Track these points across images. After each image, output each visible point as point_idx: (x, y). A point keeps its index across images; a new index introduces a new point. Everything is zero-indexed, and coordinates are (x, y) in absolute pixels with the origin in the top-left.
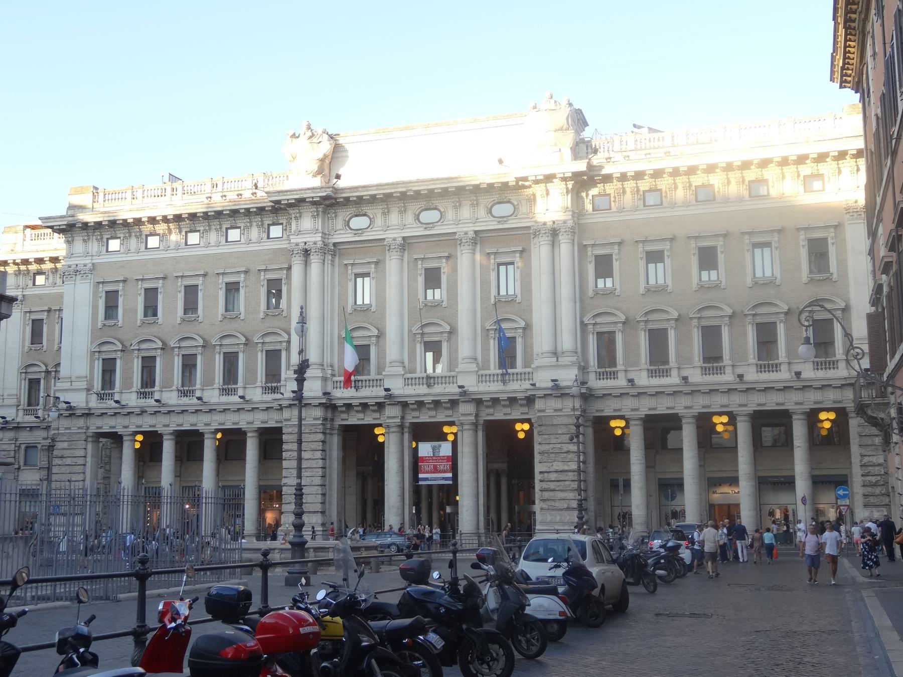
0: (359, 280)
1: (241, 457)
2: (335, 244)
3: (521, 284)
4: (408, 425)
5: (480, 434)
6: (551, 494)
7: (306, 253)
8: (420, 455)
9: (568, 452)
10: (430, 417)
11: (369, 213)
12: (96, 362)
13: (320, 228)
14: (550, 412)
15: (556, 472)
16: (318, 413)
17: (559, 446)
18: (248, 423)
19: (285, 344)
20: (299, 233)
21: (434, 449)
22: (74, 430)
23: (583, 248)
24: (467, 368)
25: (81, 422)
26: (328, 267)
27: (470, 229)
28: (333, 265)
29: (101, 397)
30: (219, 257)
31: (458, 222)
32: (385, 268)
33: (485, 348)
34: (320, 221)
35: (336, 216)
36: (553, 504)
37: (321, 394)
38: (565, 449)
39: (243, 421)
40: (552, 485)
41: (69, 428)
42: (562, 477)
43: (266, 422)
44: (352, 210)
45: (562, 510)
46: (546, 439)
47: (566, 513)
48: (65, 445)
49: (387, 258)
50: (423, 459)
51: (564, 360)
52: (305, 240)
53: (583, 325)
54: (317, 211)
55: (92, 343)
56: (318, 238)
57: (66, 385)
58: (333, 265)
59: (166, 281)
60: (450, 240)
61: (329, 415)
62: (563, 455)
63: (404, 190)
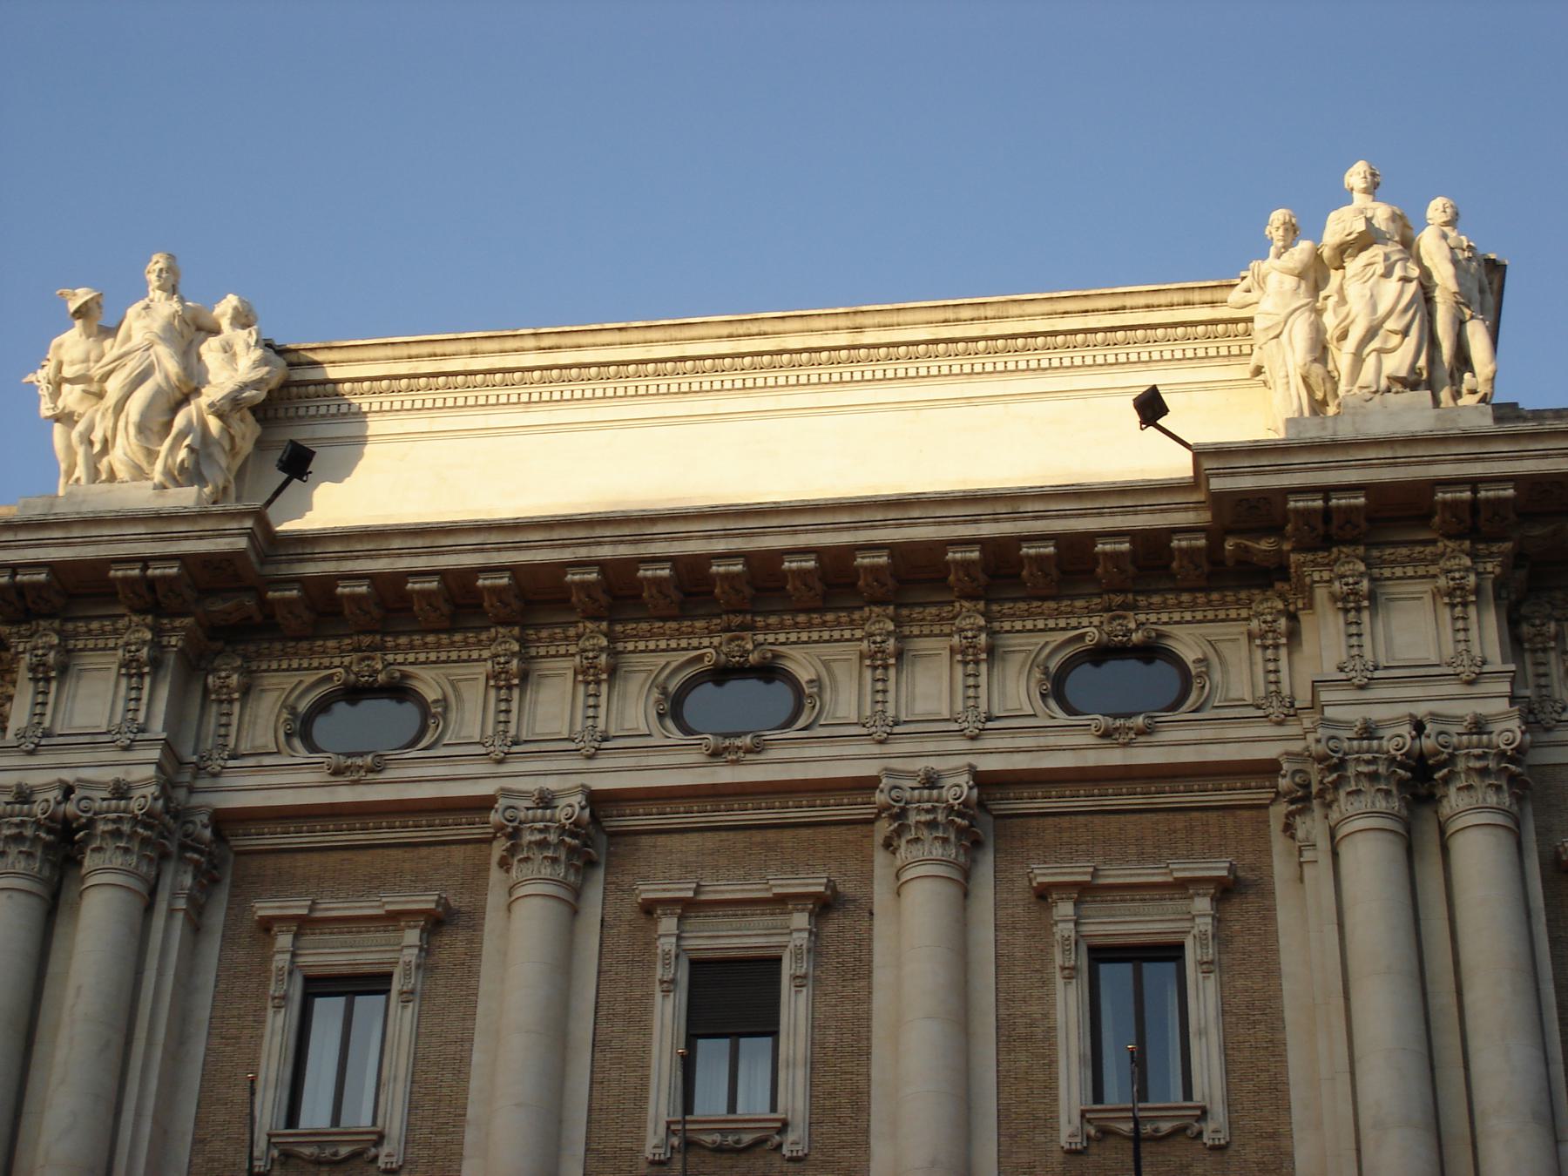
0: (328, 1011)
2: (225, 821)
3: (1227, 1049)
13: (158, 728)
26: (168, 930)
28: (196, 926)
31: (886, 730)
32: (474, 954)
35: (246, 691)
44: (340, 662)
49: (495, 899)
52: (68, 776)
54: (157, 645)
56: (141, 769)
58: (196, 926)
60: (850, 813)
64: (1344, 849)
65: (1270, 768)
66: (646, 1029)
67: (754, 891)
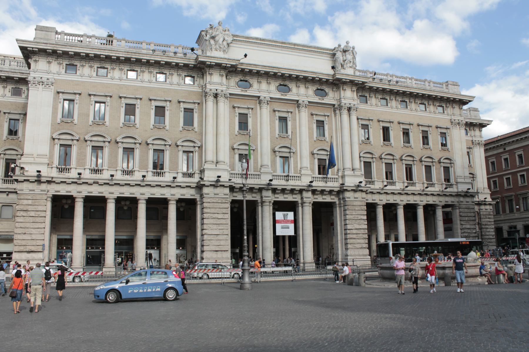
1: (134, 217)
2: (230, 94)
3: (329, 132)
6: (354, 240)
7: (216, 96)
10: (285, 198)
11: (251, 81)
12: (56, 145)
14: (352, 199)
15: (356, 229)
16: (227, 191)
17: (357, 216)
18: (172, 195)
19: (197, 148)
20: (214, 83)
21: (284, 215)
22: (37, 191)
23: (358, 119)
24: (304, 172)
25: (44, 186)
26: (226, 106)
27: (306, 100)
29: (61, 170)
30: (151, 89)
33: (312, 164)
34: (224, 78)
37: (228, 181)
38: (360, 218)
39: (166, 193)
40: (354, 236)
41: (34, 190)
43: (184, 195)
47: (361, 250)
48: (30, 202)
50: (279, 222)
51: (357, 173)
52: (217, 88)
53: (360, 157)
55: (52, 133)
57: (31, 160)
59: (112, 99)
62: (358, 221)
63: (277, 71)
64: (342, 116)
65: (334, 105)
66: (275, 124)
67: (286, 110)
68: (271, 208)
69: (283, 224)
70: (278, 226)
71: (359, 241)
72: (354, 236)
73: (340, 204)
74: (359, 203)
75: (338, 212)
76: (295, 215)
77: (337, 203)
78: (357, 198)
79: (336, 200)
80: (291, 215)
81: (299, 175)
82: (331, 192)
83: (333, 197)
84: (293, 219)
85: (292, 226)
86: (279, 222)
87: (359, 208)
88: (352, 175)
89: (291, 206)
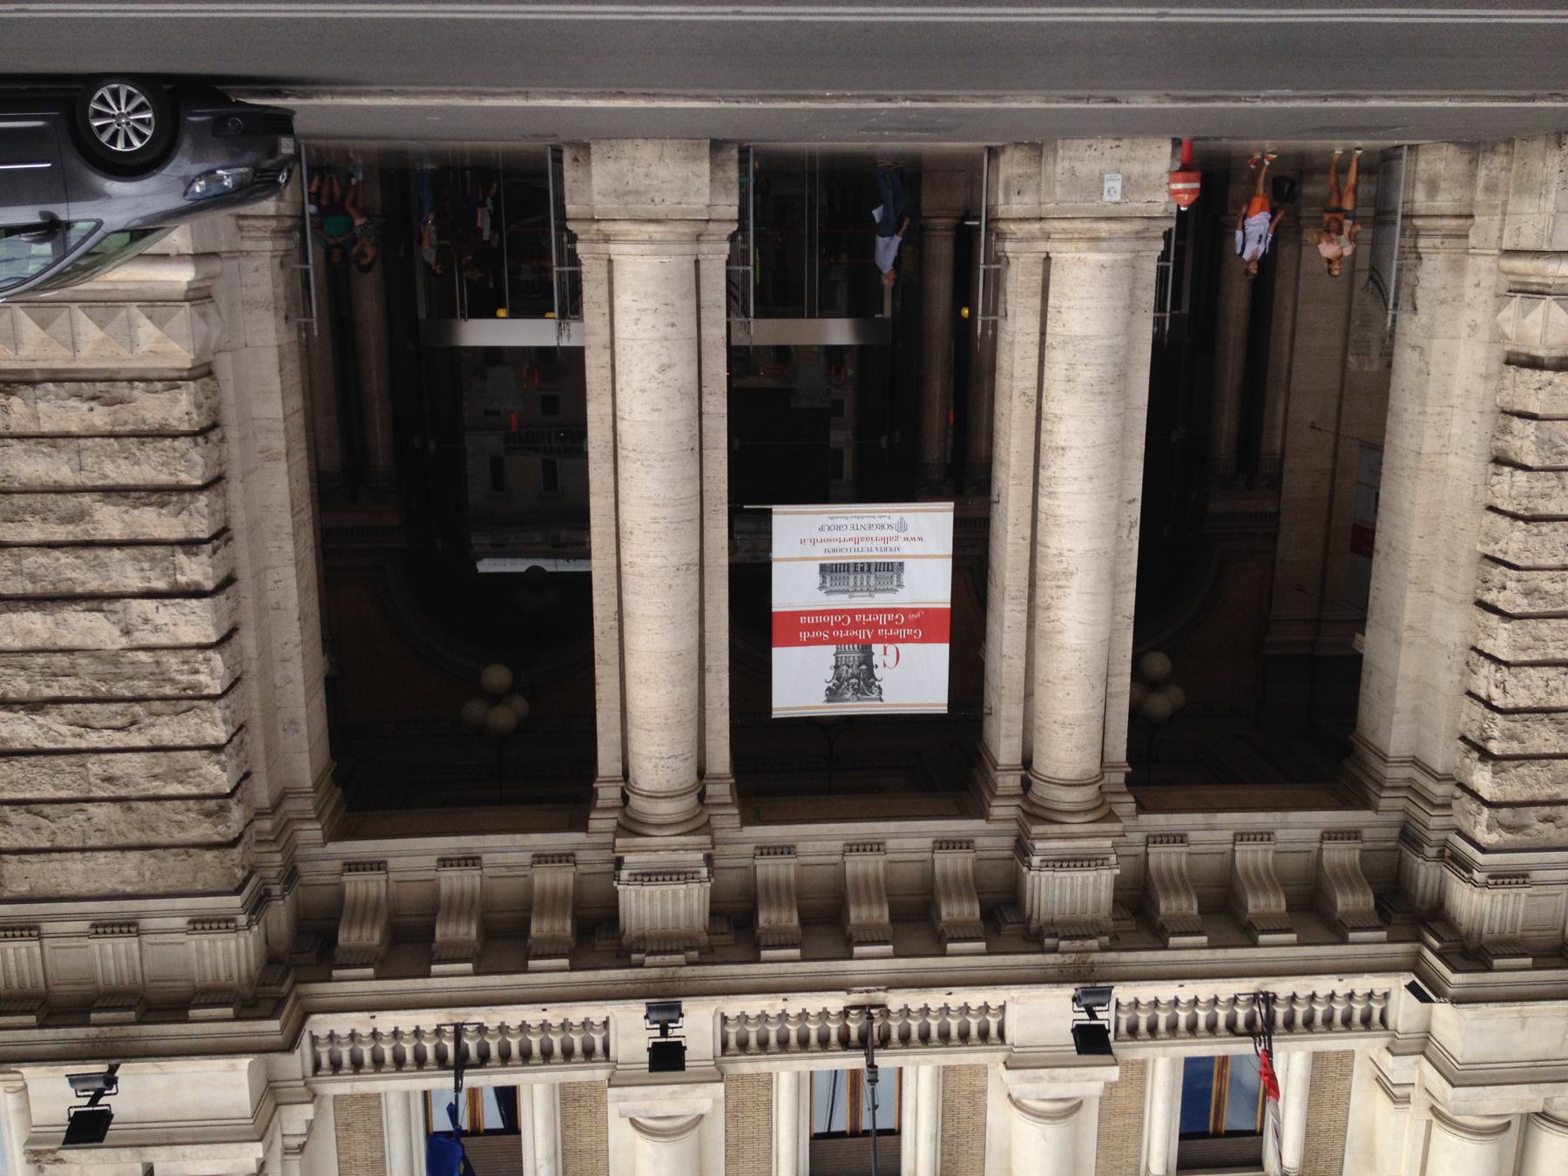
4: (1000, 809)
5: (607, 762)
6: (120, 472)
8: (946, 646)
9: (34, 706)
17: (93, 740)
21: (866, 680)
36: (100, 418)
40: (110, 520)
42: (76, 572)
45: (57, 377)
46: (181, 775)
61: (1426, 872)
62: (69, 686)
68: (1005, 747)
69: (881, 600)
70: (930, 583)
71: (60, 469)
72: (110, 520)
73: (283, 835)
74: (74, 873)
75: (301, 752)
76: (751, 675)
77: (311, 832)
78: (103, 928)
79: (327, 857)
80: (801, 682)
81: (746, 1066)
82: (409, 943)
83: (361, 886)
84: (782, 657)
85: (794, 588)
86: (920, 624)
87: (68, 828)
88: (169, 1140)
89: (782, 764)
